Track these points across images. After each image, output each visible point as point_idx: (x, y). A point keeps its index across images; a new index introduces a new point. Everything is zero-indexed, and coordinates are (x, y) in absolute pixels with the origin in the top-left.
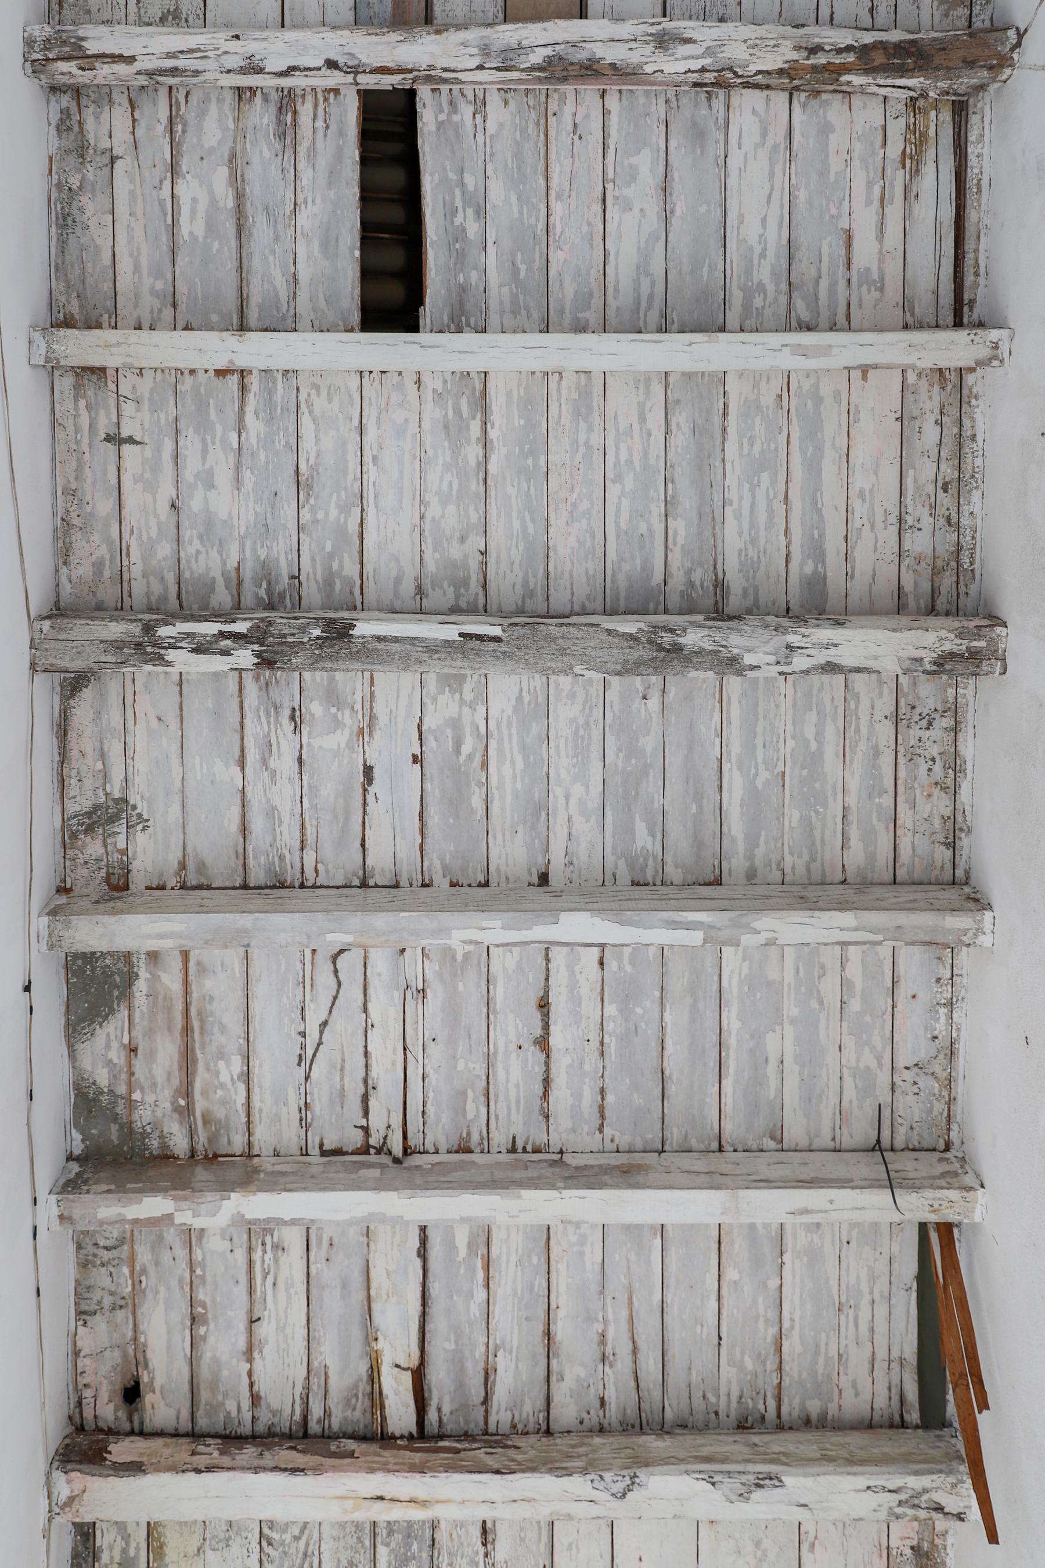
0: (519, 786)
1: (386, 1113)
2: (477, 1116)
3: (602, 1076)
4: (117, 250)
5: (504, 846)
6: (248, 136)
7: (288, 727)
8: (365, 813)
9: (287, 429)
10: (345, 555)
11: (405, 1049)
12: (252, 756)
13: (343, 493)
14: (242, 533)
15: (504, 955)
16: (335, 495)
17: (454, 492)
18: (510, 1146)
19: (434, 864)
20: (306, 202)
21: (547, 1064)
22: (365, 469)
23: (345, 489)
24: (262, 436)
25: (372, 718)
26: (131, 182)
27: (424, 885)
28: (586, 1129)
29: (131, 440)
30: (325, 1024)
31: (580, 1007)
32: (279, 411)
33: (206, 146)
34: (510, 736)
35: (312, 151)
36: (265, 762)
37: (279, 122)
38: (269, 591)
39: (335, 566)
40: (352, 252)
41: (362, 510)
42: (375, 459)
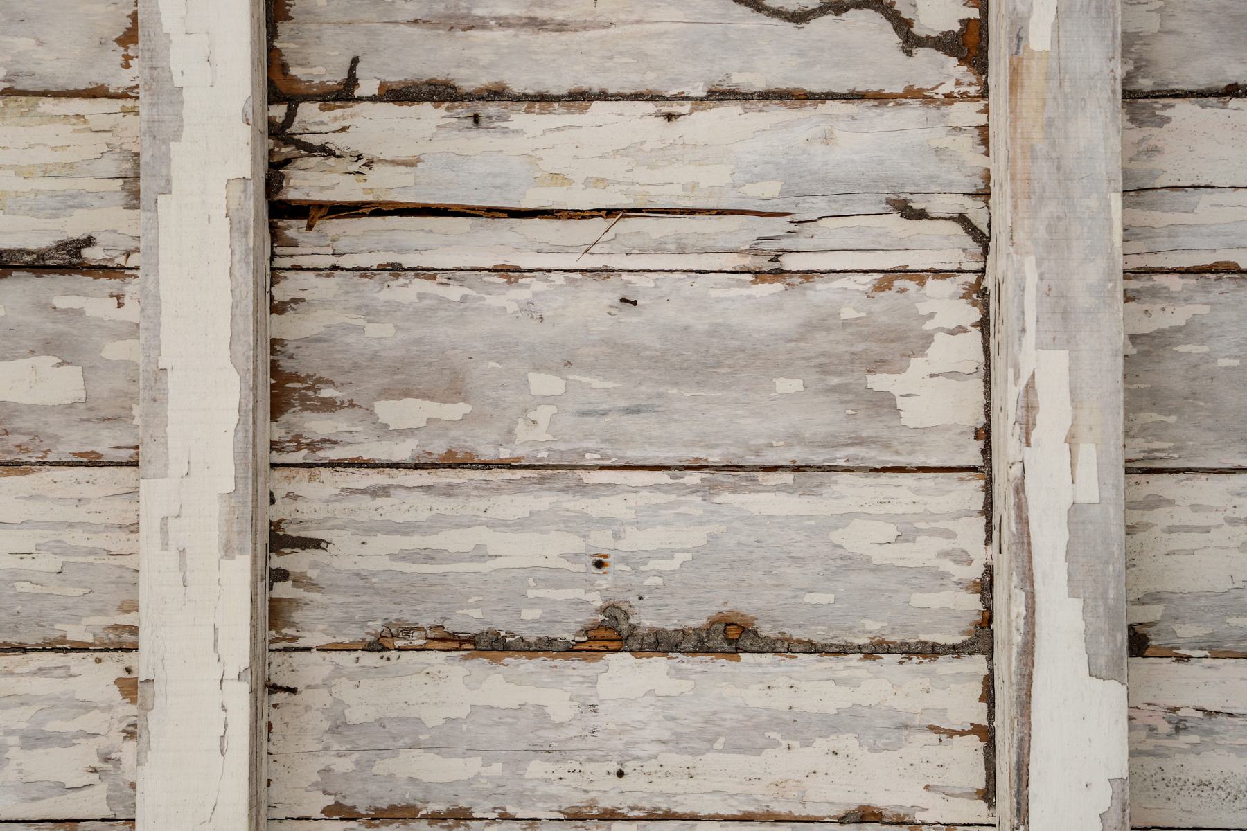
1: (404, 155)
2: (385, 432)
3: (505, 817)
5: (1232, 522)
11: (610, 213)
15: (890, 518)
18: (292, 531)
21: (546, 647)
28: (343, 765)
31: (724, 750)
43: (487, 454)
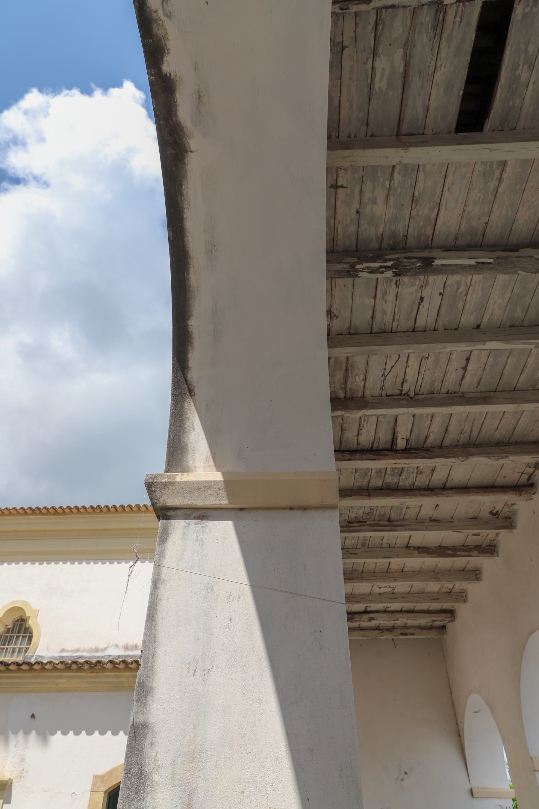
0: (478, 300)
3: (482, 375)
4: (342, 98)
7: (394, 286)
8: (418, 311)
11: (419, 372)
12: (379, 295)
13: (432, 204)
14: (386, 221)
16: (428, 204)
17: (480, 201)
22: (444, 193)
24: (400, 182)
27: (435, 330)
29: (342, 186)
30: (393, 367)
32: (409, 171)
34: (479, 286)
36: (383, 297)
39: (423, 231)
41: (439, 210)
42: (449, 189)
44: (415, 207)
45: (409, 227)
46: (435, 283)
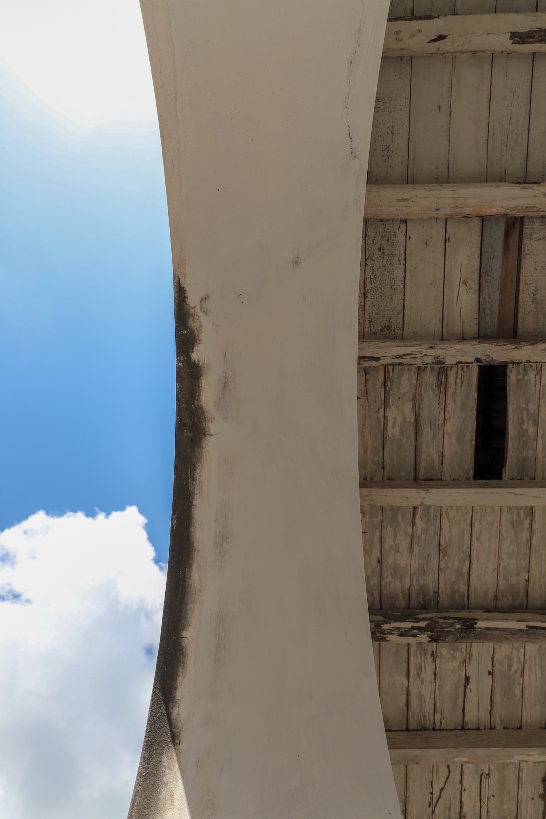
6: (423, 387)
7: (430, 659)
8: (465, 697)
9: (436, 525)
10: (461, 582)
14: (412, 573)
19: (496, 719)
20: (450, 418)
23: (463, 552)
25: (471, 655)
26: (364, 410)
27: (491, 728)
32: (432, 517)
33: (402, 392)
35: (454, 395)
37: (438, 380)
38: (424, 599)
39: (456, 587)
40: (471, 442)
43: (515, 814)
44: (444, 558)
45: (440, 581)
46: (480, 656)
